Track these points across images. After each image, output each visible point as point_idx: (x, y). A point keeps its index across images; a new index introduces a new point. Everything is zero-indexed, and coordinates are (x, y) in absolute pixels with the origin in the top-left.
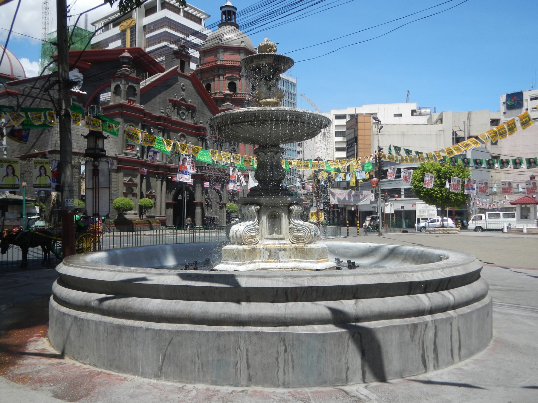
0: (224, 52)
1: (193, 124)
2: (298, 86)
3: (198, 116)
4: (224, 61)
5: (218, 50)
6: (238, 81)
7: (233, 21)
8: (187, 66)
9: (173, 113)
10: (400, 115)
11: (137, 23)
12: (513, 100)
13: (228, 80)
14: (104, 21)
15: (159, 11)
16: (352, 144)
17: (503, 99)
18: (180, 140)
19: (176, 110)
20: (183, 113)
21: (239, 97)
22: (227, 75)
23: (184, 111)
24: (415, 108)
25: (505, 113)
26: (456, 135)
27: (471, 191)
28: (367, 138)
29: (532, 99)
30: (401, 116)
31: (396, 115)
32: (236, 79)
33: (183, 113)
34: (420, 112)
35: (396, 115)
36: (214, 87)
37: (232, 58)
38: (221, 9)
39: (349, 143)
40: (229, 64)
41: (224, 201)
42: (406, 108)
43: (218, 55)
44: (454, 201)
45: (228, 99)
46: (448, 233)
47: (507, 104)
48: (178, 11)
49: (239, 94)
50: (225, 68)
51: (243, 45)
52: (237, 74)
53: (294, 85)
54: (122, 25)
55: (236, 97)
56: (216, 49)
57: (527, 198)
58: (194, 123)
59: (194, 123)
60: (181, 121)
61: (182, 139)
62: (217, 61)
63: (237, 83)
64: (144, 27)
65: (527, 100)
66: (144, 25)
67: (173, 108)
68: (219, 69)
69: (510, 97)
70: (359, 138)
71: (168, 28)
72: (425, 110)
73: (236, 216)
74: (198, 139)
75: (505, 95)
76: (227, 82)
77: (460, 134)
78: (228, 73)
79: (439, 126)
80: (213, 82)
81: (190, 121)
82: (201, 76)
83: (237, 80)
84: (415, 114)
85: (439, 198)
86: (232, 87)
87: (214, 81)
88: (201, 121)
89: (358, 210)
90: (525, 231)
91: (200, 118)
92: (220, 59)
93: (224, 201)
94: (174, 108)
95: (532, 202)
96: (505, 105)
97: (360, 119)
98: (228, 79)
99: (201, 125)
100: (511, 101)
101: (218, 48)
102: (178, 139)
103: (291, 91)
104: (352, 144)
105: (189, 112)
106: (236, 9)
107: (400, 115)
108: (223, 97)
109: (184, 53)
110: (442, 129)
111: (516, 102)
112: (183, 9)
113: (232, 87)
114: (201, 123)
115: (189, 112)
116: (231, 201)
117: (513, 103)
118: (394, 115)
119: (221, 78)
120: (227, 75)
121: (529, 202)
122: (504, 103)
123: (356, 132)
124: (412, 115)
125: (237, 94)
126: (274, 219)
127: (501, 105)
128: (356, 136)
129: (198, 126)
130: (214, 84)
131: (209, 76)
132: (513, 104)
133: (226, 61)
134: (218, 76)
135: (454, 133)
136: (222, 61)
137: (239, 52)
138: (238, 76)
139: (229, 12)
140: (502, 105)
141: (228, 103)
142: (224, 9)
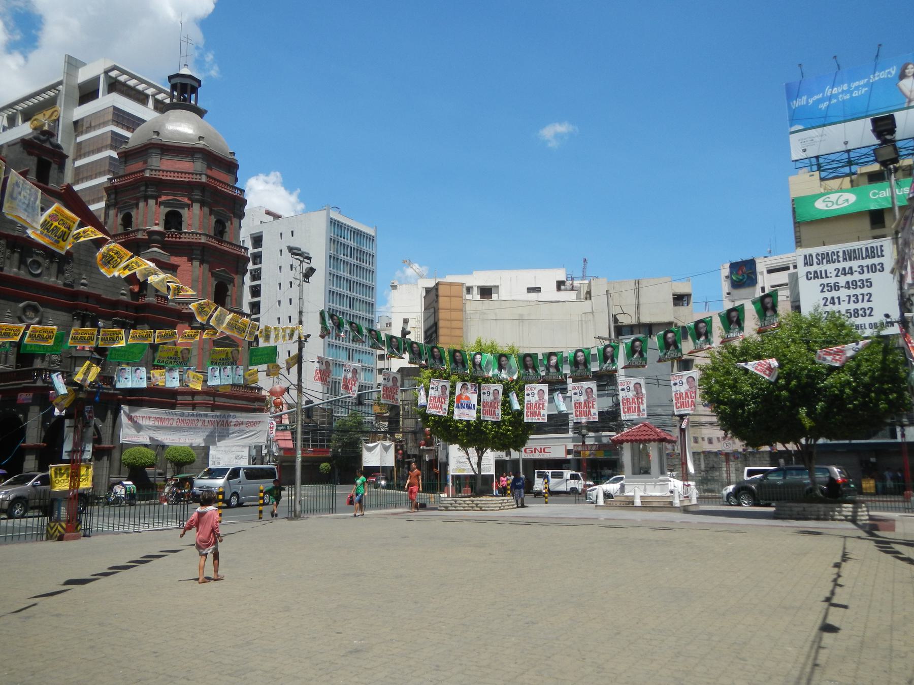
0: (162, 154)
1: (62, 287)
2: (379, 242)
3: (76, 271)
4: (159, 171)
5: (150, 151)
6: (186, 209)
8: (56, 171)
9: (8, 262)
10: (537, 290)
11: (62, 115)
12: (741, 272)
13: (165, 207)
14: (6, 111)
15: (103, 95)
16: (431, 335)
17: (726, 271)
18: (24, 317)
19: (16, 256)
20: (34, 262)
21: (185, 239)
22: (164, 198)
23: (40, 259)
24: (564, 279)
25: (729, 294)
26: (616, 320)
27: (466, 411)
28: (455, 324)
29: (770, 271)
30: (540, 291)
31: (530, 290)
32: (183, 206)
33: (34, 262)
34: (572, 285)
35: (530, 290)
36: (137, 219)
37: (177, 166)
38: (169, 81)
39: (429, 333)
40: (168, 178)
42: (547, 278)
43: (149, 160)
44: (493, 438)
45: (155, 241)
46: (481, 510)
47: (732, 279)
48: (144, 99)
49: (186, 233)
50: (159, 186)
51: (201, 144)
52: (184, 196)
53: (371, 239)
54: (35, 120)
55: (178, 240)
56: (147, 149)
57: (646, 428)
58: (65, 285)
59: (65, 285)
60: (29, 278)
61: (30, 314)
62: (143, 171)
63: (185, 213)
64: (76, 123)
65: (762, 273)
66: (75, 119)
67: (8, 252)
68: (147, 186)
69: (734, 266)
70: (441, 324)
71: (117, 126)
72: (581, 282)
73: (160, 474)
74: (74, 315)
75: (729, 264)
76: (164, 210)
77: (624, 320)
78: (166, 194)
79: (587, 305)
80: (135, 210)
81: (53, 279)
82: (115, 199)
83: (183, 208)
84: (563, 287)
85: (462, 430)
86: (173, 220)
87: (138, 209)
88: (83, 281)
89: (437, 459)
90: (638, 502)
91: (80, 274)
92: (153, 168)
94: (13, 252)
95: (651, 437)
96: (729, 281)
98: (165, 204)
99: (82, 288)
100: (737, 274)
101: (150, 148)
102: (19, 313)
103: (364, 249)
104: (431, 335)
105: (52, 262)
106: (199, 82)
107: (537, 290)
108: (147, 237)
109: (48, 145)
110: (591, 311)
111: (745, 276)
112: (153, 96)
113: (173, 220)
114: (83, 284)
115: (52, 262)
117: (741, 278)
118: (528, 289)
119: (152, 202)
120: (164, 198)
121: (646, 437)
122: (727, 277)
123: (436, 314)
124: (559, 289)
125: (183, 233)
127: (723, 281)
128: (436, 321)
129: (75, 289)
130: (137, 213)
131: (131, 199)
132: (742, 280)
133: (163, 171)
134: (146, 199)
136: (156, 170)
137: (192, 157)
138: (186, 200)
140: (725, 281)
141: (155, 249)
142: (174, 81)
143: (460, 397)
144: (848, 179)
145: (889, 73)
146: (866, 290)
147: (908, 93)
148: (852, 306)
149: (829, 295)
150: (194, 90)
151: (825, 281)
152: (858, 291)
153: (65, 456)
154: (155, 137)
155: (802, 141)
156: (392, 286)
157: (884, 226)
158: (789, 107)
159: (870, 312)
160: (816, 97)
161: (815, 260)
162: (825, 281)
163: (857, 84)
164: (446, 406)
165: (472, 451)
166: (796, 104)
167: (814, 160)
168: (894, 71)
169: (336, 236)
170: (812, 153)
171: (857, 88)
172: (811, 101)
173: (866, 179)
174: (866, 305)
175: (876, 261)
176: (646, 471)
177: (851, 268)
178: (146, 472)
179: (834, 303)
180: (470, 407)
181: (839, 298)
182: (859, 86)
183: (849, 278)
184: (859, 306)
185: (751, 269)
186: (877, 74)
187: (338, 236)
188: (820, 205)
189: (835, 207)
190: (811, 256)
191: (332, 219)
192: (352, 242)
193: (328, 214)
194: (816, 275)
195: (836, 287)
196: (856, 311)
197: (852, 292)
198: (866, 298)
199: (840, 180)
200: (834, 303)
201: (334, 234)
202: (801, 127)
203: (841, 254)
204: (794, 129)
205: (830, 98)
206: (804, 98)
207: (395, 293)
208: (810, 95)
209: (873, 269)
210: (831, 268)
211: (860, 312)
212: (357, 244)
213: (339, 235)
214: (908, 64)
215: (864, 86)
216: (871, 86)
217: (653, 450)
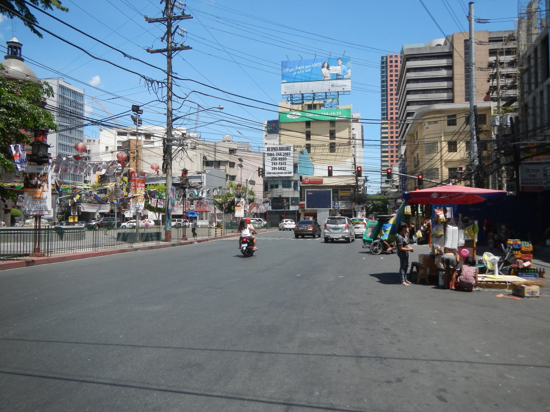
7: (19, 56)
25: (266, 136)
26: (206, 159)
41: (9, 208)
53: (82, 96)
72: (193, 134)
73: (19, 219)
77: (209, 159)
93: (9, 208)
97: (131, 141)
106: (22, 45)
116: (14, 207)
135: (205, 158)
139: (15, 47)
143: (159, 203)
144: (301, 105)
145: (319, 64)
147: (324, 74)
148: (280, 166)
150: (20, 49)
151: (273, 157)
153: (72, 215)
154: (6, 74)
155: (286, 87)
156: (100, 130)
159: (284, 169)
161: (271, 149)
162: (273, 157)
163: (307, 67)
164: (156, 204)
165: (157, 214)
167: (289, 96)
168: (320, 64)
169: (62, 94)
170: (289, 92)
171: (307, 68)
173: (307, 107)
174: (284, 166)
175: (288, 152)
176: (202, 219)
177: (281, 153)
178: (15, 219)
179: (275, 165)
180: (162, 205)
181: (276, 163)
182: (308, 68)
183: (280, 157)
184: (282, 166)
185: (276, 125)
186: (314, 64)
187: (63, 94)
190: (269, 148)
191: (60, 85)
192: (71, 98)
193: (58, 82)
194: (271, 155)
196: (281, 168)
197: (280, 161)
198: (284, 163)
199: (298, 105)
200: (275, 165)
201: (61, 93)
202: (286, 81)
203: (278, 148)
204: (283, 81)
206: (288, 69)
207: (101, 133)
208: (290, 68)
209: (287, 154)
210: (275, 153)
211: (282, 168)
212: (74, 98)
213: (64, 93)
215: (309, 68)
216: (312, 68)
217: (204, 214)
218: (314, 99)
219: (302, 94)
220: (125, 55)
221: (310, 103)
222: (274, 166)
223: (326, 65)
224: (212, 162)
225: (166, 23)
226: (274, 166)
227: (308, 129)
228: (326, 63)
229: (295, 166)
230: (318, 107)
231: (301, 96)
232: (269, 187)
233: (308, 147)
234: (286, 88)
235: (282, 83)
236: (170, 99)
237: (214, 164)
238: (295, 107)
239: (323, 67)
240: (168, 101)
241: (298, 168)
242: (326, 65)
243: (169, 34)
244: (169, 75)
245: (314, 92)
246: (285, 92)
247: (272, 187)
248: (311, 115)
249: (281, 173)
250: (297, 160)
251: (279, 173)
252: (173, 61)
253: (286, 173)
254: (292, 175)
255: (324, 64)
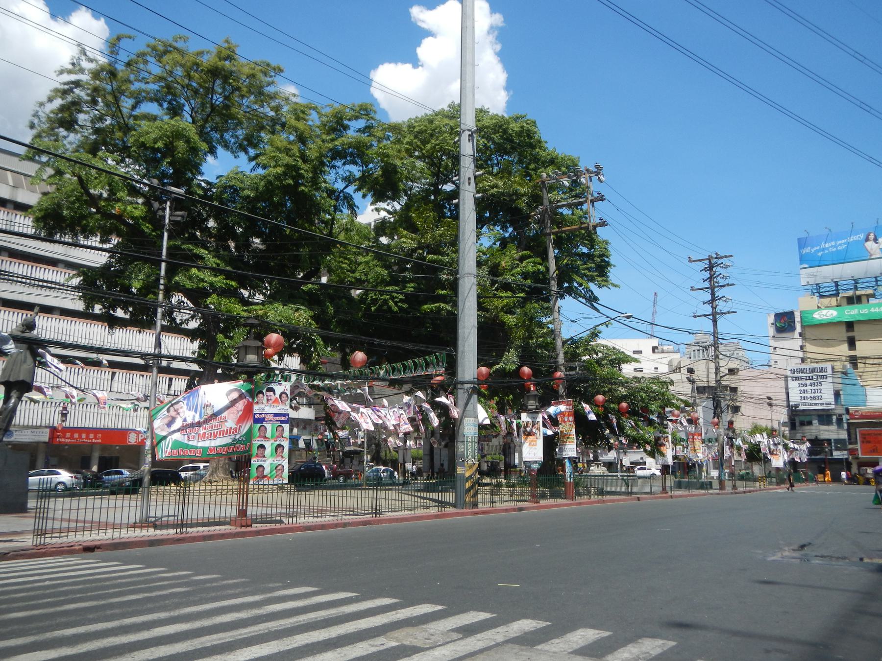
17: (771, 319)
25: (774, 337)
34: (663, 350)
69: (779, 316)
84: (656, 350)
96: (774, 327)
122: (772, 324)
124: (654, 352)
126: (598, 467)
144: (834, 299)
145: (859, 237)
146: (819, 387)
148: (813, 395)
149: (802, 389)
152: (816, 388)
157: (853, 331)
158: (799, 251)
160: (816, 248)
163: (840, 242)
166: (804, 251)
168: (862, 236)
170: (812, 281)
171: (840, 245)
172: (813, 251)
173: (845, 301)
184: (816, 395)
188: (816, 316)
189: (825, 318)
195: (806, 385)
196: (814, 397)
197: (813, 388)
202: (807, 266)
204: (803, 266)
205: (823, 250)
206: (809, 248)
208: (812, 247)
209: (823, 377)
214: (870, 233)
215: (844, 244)
218: (856, 288)
219: (836, 282)
220: (690, 333)
221: (850, 293)
222: (803, 395)
223: (872, 236)
224: (704, 388)
225: (710, 291)
226: (803, 395)
227: (850, 334)
228: (872, 234)
229: (837, 394)
230: (864, 299)
231: (834, 285)
232: (797, 424)
233: (854, 361)
234: (808, 275)
235: (802, 269)
236: (717, 357)
237: (707, 390)
238: (826, 301)
239: (867, 240)
240: (715, 359)
241: (842, 397)
242: (872, 236)
243: (714, 299)
244: (715, 337)
245: (855, 278)
246: (808, 282)
247: (802, 424)
248: (852, 313)
249: (816, 404)
250: (839, 387)
251: (811, 405)
252: (720, 323)
253: (823, 404)
254: (832, 407)
255: (869, 235)
